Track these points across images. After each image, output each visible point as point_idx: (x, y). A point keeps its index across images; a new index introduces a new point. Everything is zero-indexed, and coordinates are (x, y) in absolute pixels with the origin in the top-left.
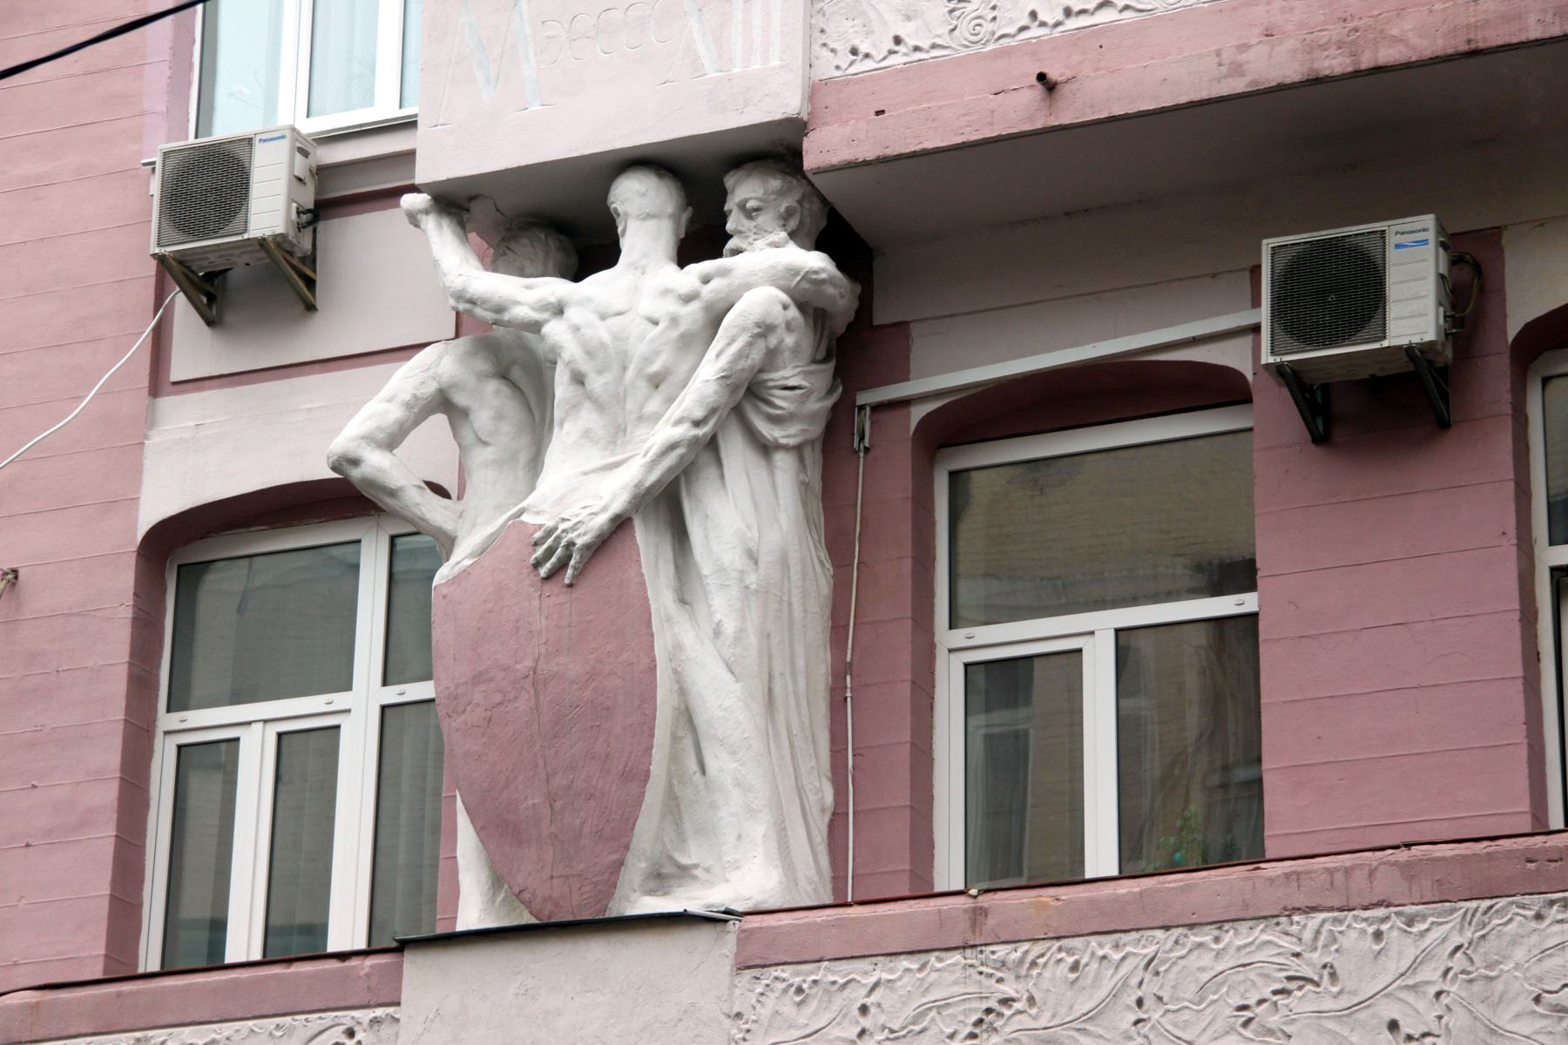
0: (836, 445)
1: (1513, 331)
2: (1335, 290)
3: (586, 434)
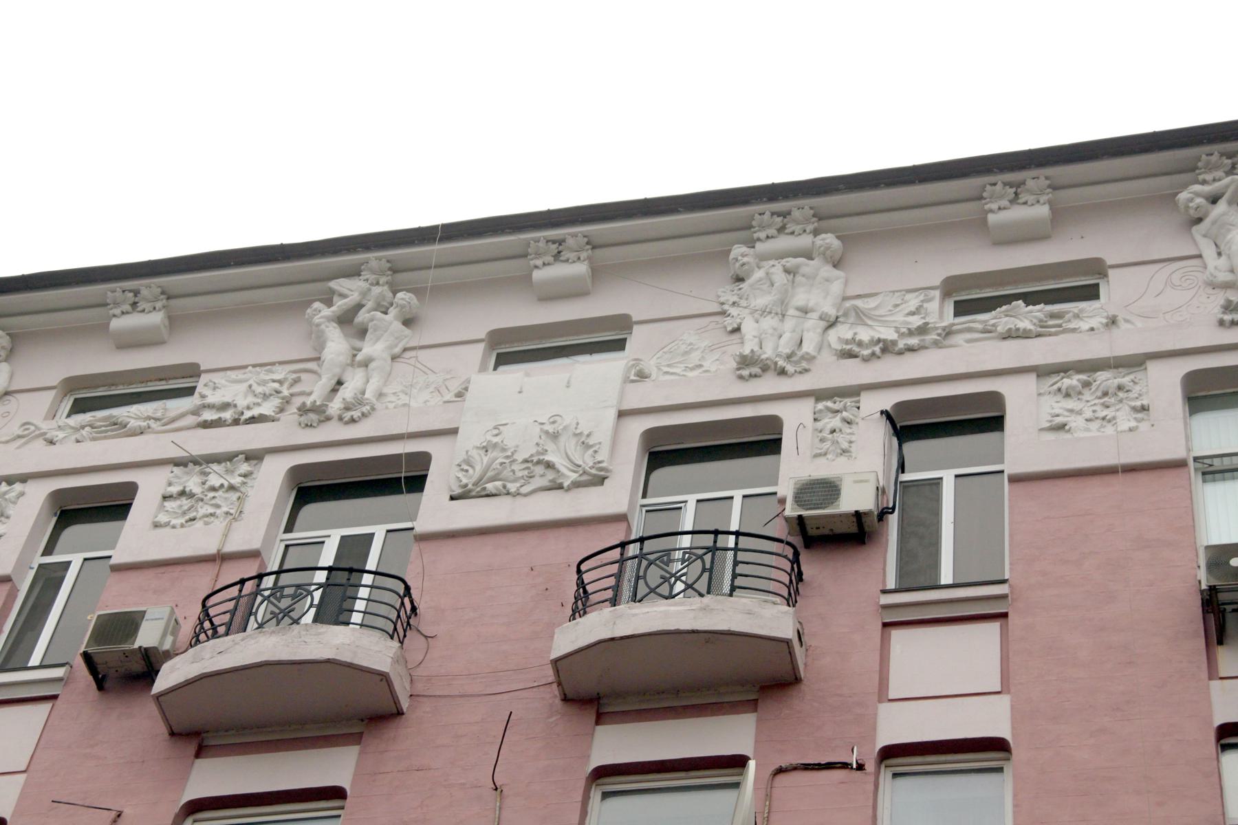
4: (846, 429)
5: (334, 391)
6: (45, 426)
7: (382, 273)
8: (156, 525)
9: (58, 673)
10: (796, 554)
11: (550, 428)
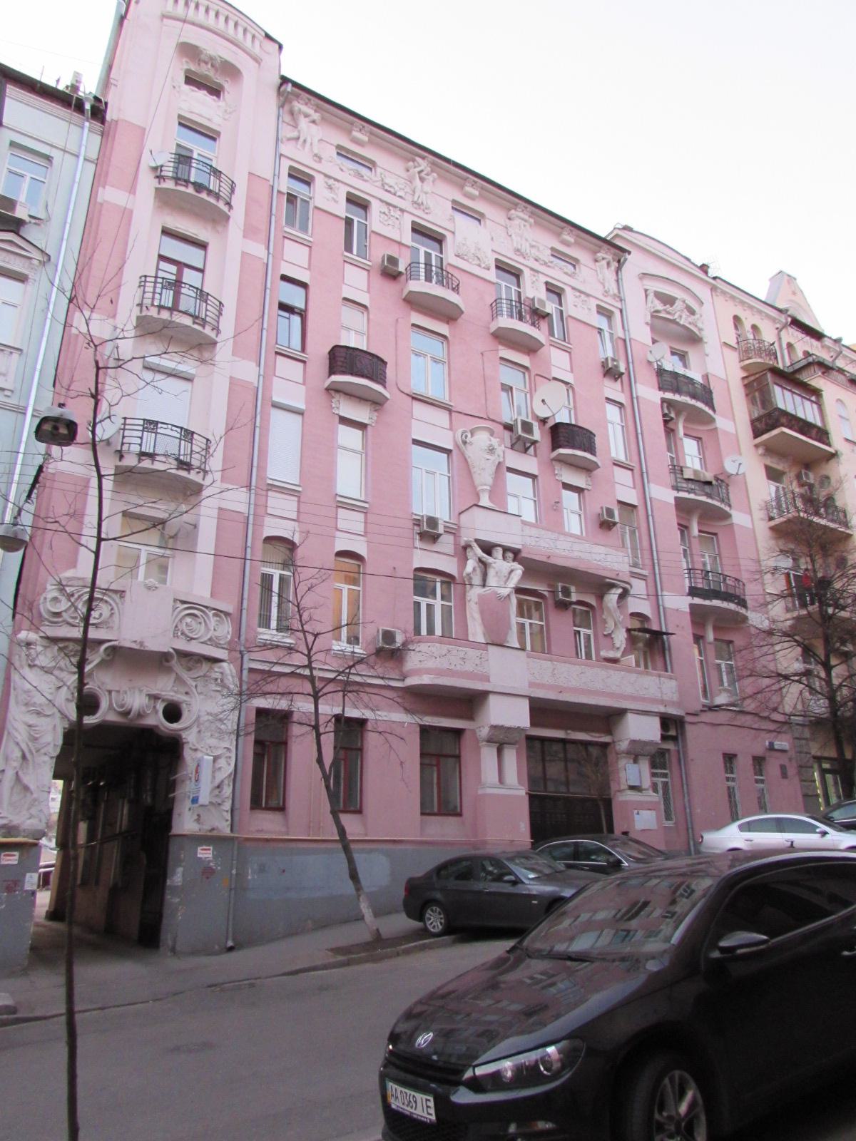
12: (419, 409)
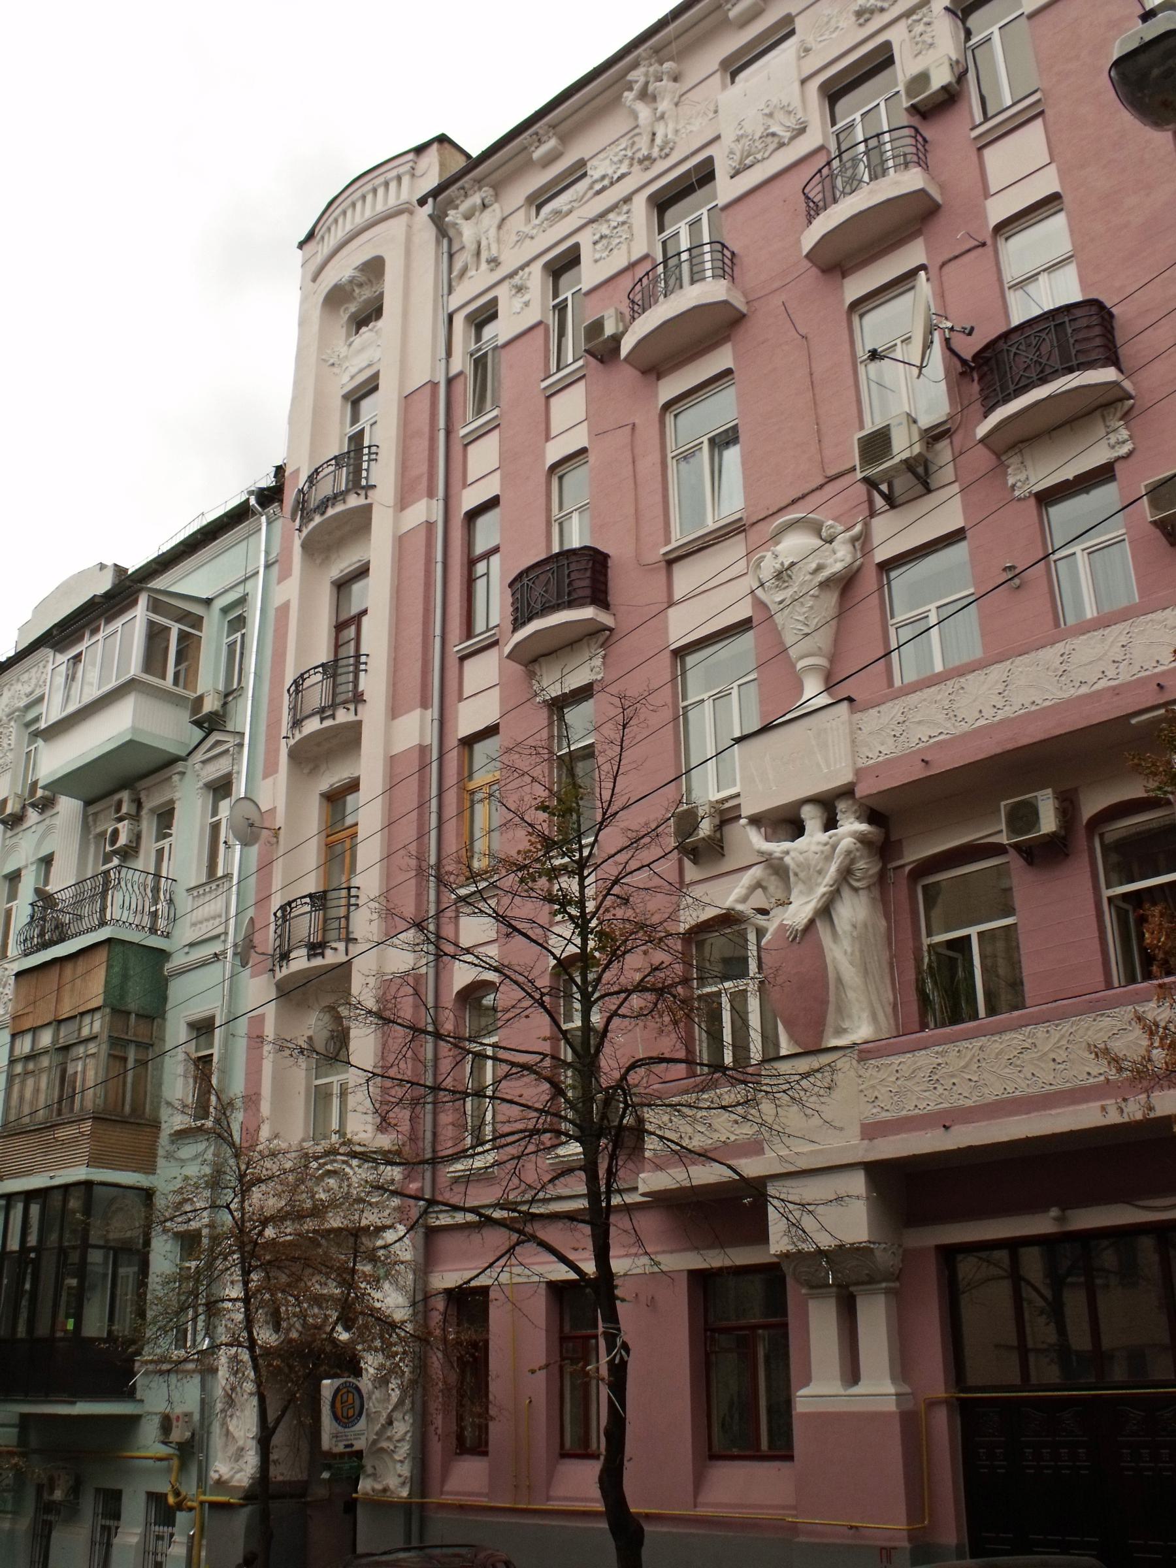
0: (882, 881)
1: (1084, 822)
2: (1024, 817)
3: (801, 892)
4: (929, 29)
5: (653, 140)
6: (526, 229)
7: (650, 57)
8: (596, 261)
9: (580, 363)
10: (916, 130)
11: (767, 111)
12: (686, 578)
